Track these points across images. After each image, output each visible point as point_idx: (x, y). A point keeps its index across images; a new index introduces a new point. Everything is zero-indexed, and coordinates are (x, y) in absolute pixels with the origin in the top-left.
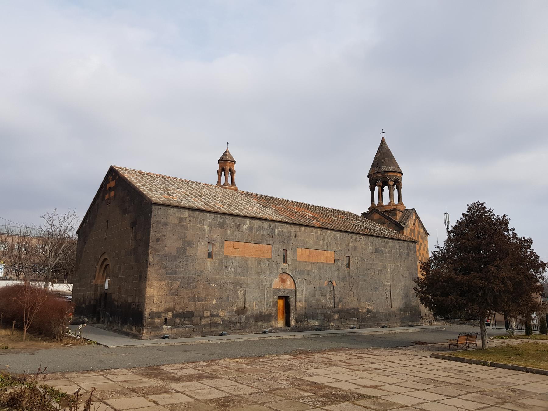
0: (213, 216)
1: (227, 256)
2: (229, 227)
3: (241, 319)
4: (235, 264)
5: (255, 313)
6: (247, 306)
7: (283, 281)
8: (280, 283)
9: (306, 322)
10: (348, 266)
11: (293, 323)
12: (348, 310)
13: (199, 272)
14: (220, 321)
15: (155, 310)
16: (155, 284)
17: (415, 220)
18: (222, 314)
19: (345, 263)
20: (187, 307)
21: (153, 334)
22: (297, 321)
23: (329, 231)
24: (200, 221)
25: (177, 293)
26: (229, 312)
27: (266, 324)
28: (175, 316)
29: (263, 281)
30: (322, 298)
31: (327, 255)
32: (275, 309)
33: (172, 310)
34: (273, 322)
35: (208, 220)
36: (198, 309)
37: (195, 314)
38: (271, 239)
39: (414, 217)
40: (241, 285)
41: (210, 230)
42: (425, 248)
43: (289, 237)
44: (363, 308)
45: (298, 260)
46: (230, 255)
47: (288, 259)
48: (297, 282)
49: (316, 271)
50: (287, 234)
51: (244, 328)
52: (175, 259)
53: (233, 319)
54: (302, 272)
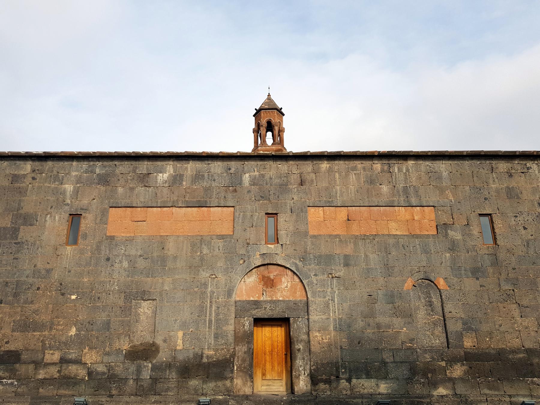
0: (85, 165)
1: (112, 238)
2: (122, 181)
3: (139, 371)
4: (133, 252)
6: (159, 341)
7: (269, 283)
9: (344, 383)
12: (500, 356)
13: (43, 272)
14: (82, 373)
18: (91, 357)
20: (7, 343)
22: (314, 379)
23: (411, 163)
24: (57, 176)
26: (108, 354)
27: (212, 385)
29: (205, 285)
30: (397, 322)
31: (408, 217)
32: (245, 349)
34: (238, 382)
35: (74, 174)
36: (32, 347)
37: (24, 357)
38: (230, 196)
40: (144, 295)
41: (76, 192)
43: (283, 188)
45: (312, 232)
46: (121, 234)
47: (282, 233)
48: (311, 283)
49: (371, 256)
50: (277, 181)
53: (119, 370)
54: (326, 260)
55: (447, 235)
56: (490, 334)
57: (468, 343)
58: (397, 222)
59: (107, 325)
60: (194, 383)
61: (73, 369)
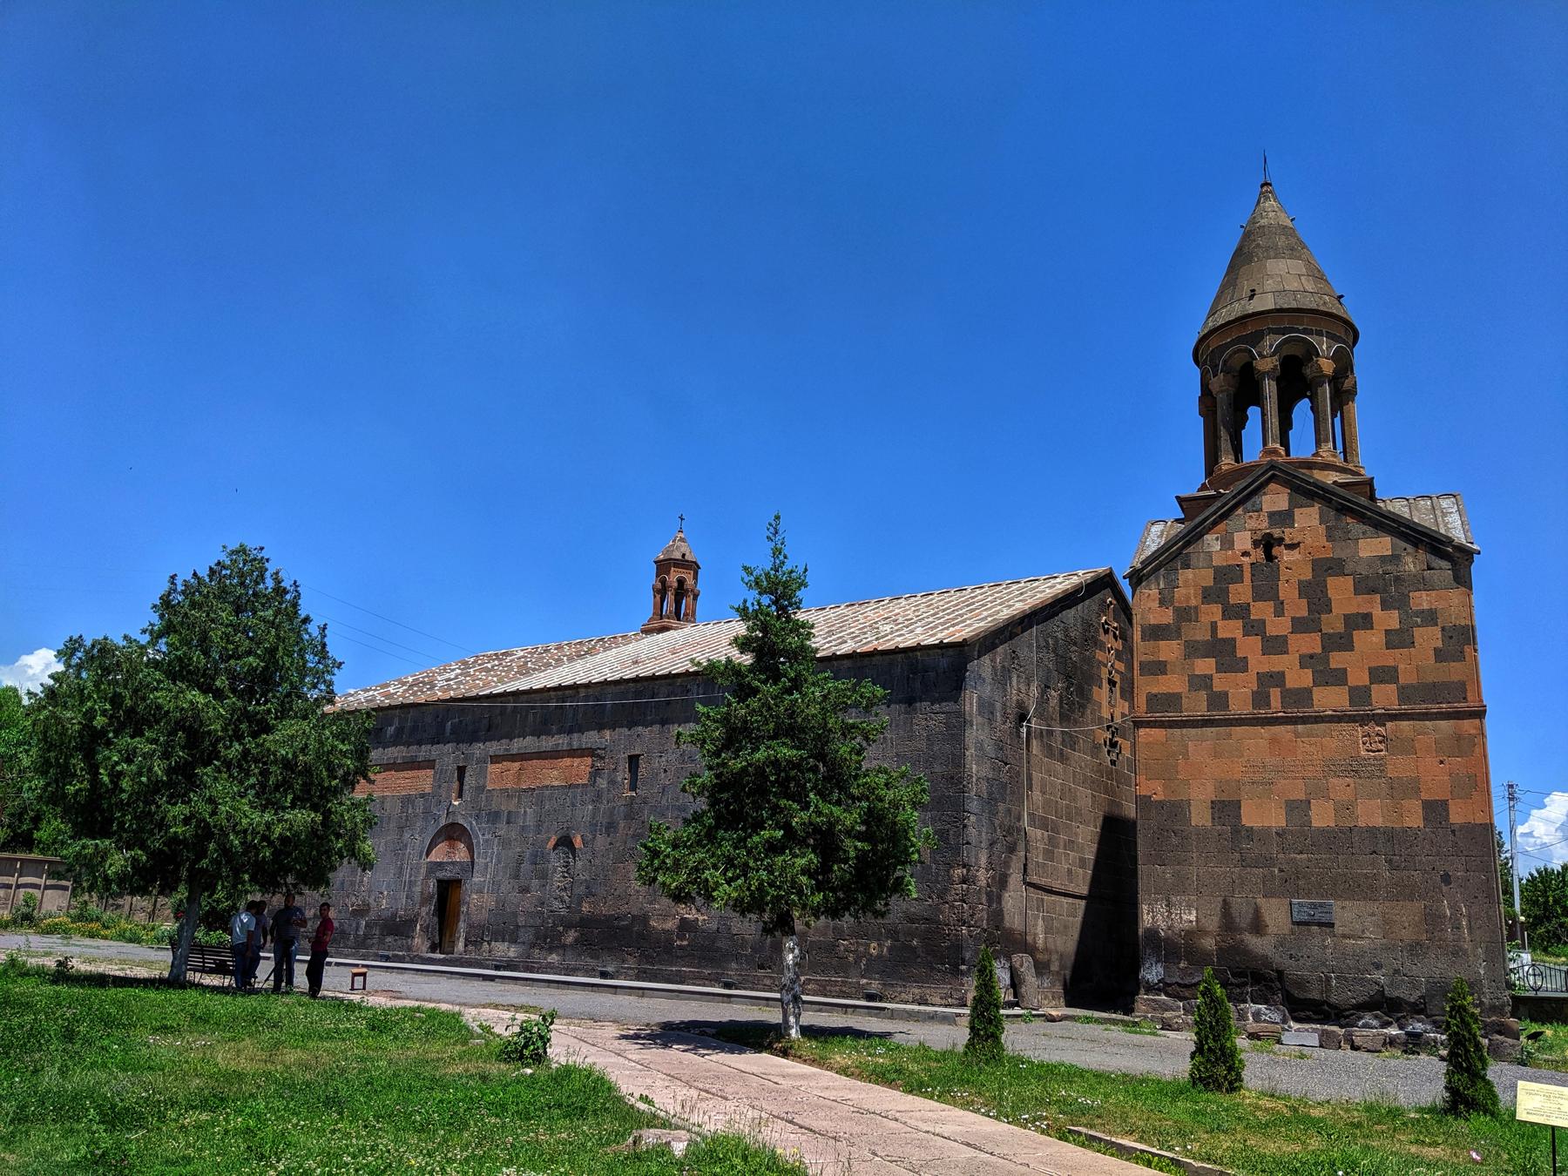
44: (665, 916)
54: (494, 817)
57: (586, 908)
60: (389, 939)
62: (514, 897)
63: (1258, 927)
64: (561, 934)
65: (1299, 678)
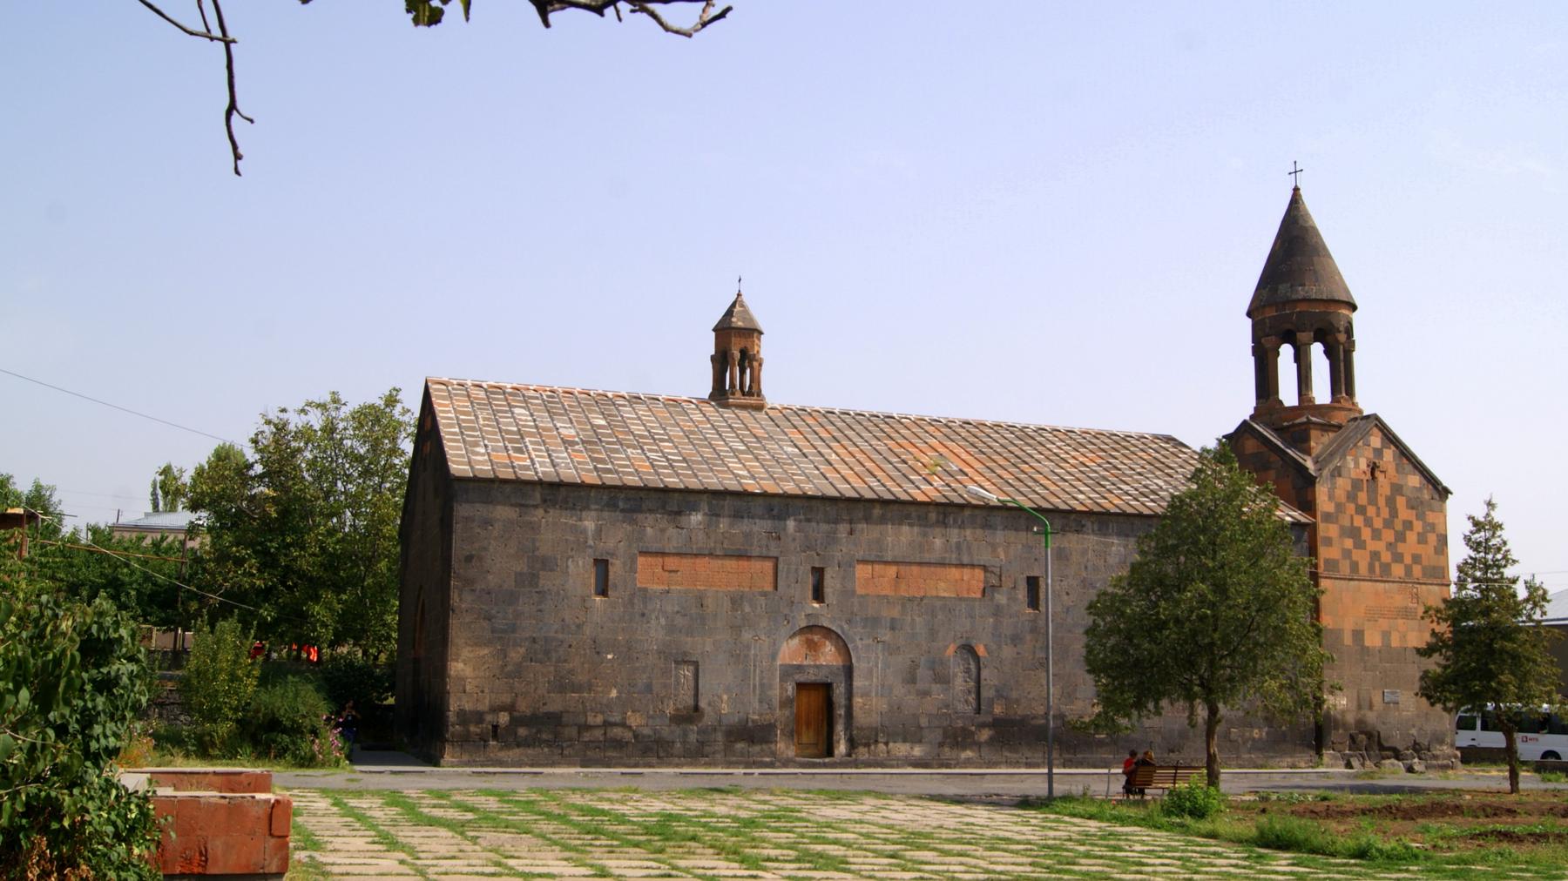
1: (645, 590)
3: (685, 734)
4: (669, 609)
5: (725, 721)
6: (703, 704)
7: (812, 646)
8: (804, 651)
9: (882, 746)
10: (1034, 602)
11: (841, 748)
12: (1023, 722)
14: (628, 735)
15: (468, 707)
16: (466, 653)
17: (1379, 452)
18: (634, 720)
19: (1022, 593)
21: (465, 758)
22: (852, 744)
25: (518, 673)
27: (757, 748)
28: (516, 721)
29: (748, 647)
30: (936, 688)
33: (510, 708)
38: (773, 544)
39: (1376, 440)
41: (599, 530)
42: (1432, 538)
45: (860, 591)
47: (828, 590)
48: (856, 648)
51: (697, 753)
52: (512, 598)
53: (666, 732)
54: (873, 622)
55: (992, 599)
56: (1017, 701)
57: (998, 710)
58: (945, 584)
59: (649, 688)
60: (739, 746)
61: (617, 732)
62: (911, 701)
63: (1371, 707)
64: (973, 733)
65: (1386, 557)
